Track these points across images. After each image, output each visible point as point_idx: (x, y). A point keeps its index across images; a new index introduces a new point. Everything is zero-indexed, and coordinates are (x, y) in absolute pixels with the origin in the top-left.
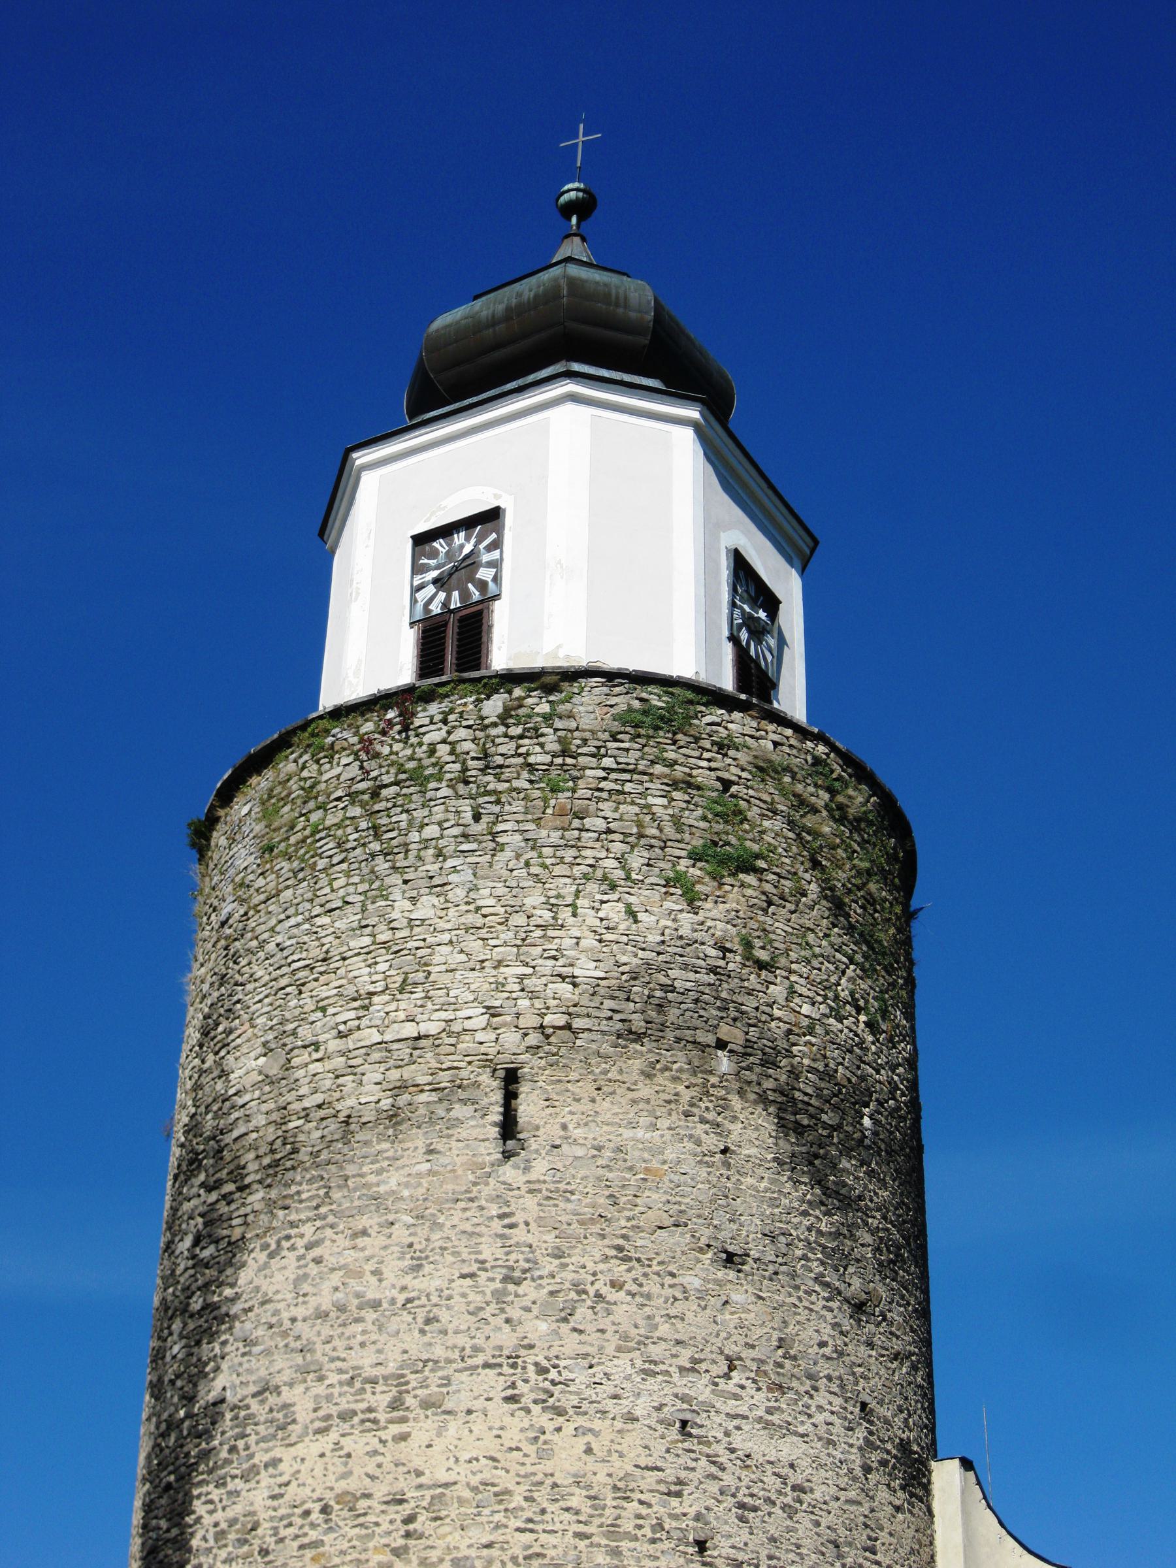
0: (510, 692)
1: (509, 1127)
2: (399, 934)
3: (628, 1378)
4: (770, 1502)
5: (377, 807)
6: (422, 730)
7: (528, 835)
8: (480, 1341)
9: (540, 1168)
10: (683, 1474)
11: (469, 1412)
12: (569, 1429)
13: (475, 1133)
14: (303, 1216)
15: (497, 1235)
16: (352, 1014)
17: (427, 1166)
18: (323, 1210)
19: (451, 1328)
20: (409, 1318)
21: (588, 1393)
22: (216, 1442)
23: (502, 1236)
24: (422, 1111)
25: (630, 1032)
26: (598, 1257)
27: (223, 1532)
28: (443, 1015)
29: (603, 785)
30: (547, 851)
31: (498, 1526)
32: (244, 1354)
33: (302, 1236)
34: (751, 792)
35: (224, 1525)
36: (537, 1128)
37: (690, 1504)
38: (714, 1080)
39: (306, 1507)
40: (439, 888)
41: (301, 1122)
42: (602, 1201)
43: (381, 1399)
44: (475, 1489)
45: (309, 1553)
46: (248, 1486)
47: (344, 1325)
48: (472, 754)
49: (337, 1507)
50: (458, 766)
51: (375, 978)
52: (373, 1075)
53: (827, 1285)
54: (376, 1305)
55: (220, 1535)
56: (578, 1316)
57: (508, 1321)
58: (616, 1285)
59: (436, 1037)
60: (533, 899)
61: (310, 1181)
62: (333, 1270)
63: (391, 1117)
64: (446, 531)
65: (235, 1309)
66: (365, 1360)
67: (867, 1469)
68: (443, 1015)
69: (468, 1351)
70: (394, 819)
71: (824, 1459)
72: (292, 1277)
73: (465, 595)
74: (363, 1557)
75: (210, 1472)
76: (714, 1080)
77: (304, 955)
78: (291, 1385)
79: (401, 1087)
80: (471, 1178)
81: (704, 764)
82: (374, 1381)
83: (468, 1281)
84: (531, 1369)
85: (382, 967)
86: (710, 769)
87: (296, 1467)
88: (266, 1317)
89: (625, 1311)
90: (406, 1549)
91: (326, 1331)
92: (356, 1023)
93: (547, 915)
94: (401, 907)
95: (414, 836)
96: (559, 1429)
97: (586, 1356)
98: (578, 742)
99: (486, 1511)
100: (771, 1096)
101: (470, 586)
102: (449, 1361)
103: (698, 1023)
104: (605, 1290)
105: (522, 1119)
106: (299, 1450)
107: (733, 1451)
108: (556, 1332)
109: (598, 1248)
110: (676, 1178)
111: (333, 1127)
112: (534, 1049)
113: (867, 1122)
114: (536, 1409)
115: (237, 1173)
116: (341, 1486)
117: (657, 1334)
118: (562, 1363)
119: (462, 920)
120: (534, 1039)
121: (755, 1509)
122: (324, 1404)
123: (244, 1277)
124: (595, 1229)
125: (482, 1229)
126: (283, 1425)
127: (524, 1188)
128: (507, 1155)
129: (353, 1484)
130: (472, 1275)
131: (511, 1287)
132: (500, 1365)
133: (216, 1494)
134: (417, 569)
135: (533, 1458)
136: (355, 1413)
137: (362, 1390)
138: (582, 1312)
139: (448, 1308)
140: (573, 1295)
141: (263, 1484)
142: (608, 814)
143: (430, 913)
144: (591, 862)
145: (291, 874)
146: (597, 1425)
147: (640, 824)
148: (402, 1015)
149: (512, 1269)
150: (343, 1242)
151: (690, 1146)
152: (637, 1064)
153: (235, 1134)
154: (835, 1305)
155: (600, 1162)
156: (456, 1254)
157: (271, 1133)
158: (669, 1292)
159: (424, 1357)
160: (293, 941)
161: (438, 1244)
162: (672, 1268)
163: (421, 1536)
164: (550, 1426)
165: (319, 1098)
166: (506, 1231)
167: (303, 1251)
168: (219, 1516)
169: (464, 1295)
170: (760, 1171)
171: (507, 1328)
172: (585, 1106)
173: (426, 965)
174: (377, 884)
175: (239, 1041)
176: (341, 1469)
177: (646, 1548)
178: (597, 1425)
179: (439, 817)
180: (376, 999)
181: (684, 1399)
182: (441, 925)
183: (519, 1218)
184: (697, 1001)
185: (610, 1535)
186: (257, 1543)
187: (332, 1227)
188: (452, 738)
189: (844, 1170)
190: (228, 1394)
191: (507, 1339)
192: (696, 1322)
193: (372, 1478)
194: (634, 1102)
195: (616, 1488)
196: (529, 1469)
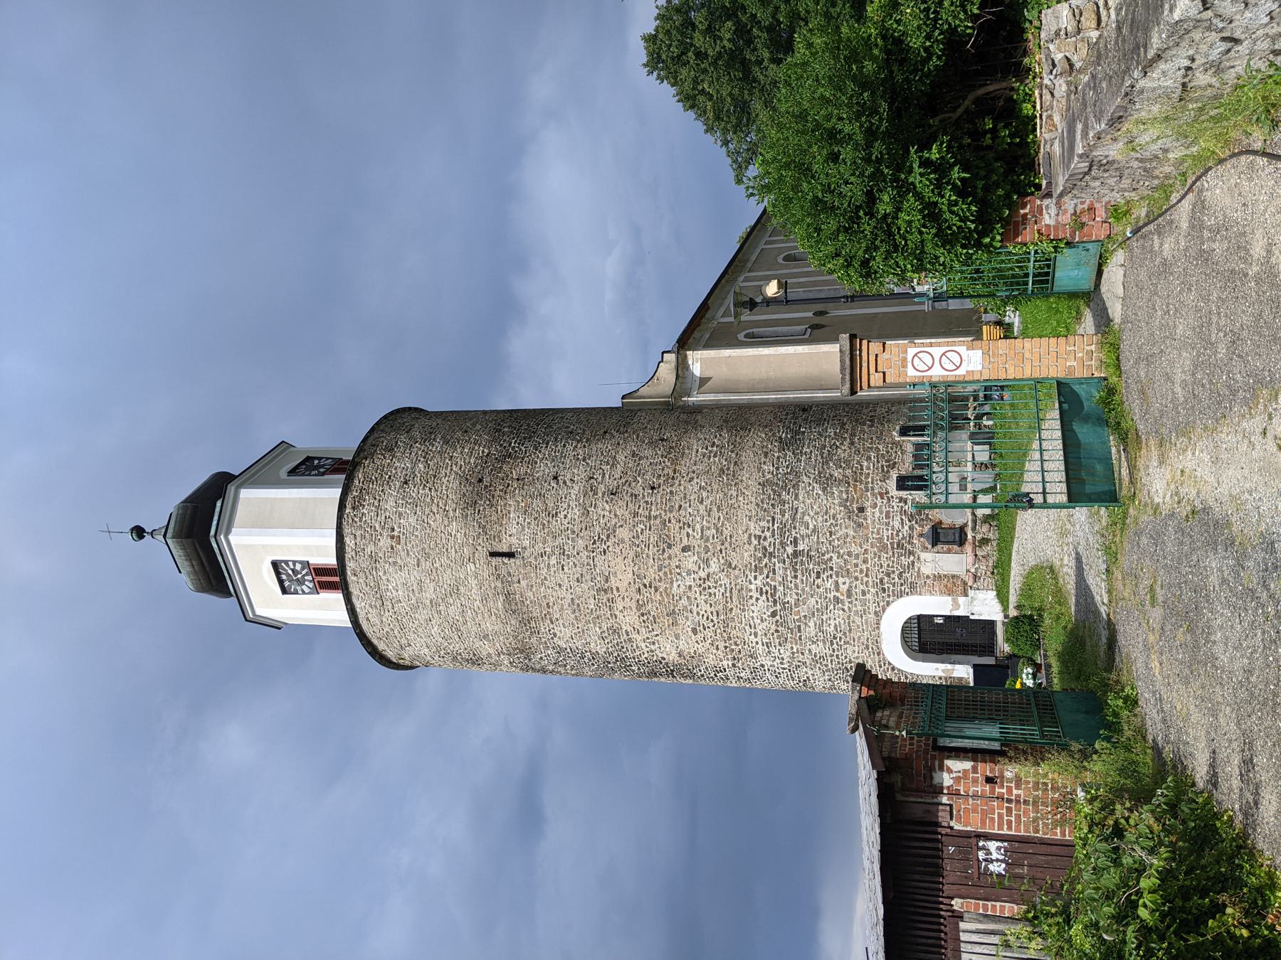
1: (510, 555)
15: (549, 558)
16: (469, 611)
44: (635, 564)
58: (566, 517)
64: (281, 582)
90: (655, 587)
105: (508, 550)
107: (621, 477)
108: (582, 538)
114: (608, 544)
116: (634, 609)
126: (615, 631)
129: (634, 605)
131: (566, 553)
134: (296, 593)
176: (629, 610)
193: (631, 599)
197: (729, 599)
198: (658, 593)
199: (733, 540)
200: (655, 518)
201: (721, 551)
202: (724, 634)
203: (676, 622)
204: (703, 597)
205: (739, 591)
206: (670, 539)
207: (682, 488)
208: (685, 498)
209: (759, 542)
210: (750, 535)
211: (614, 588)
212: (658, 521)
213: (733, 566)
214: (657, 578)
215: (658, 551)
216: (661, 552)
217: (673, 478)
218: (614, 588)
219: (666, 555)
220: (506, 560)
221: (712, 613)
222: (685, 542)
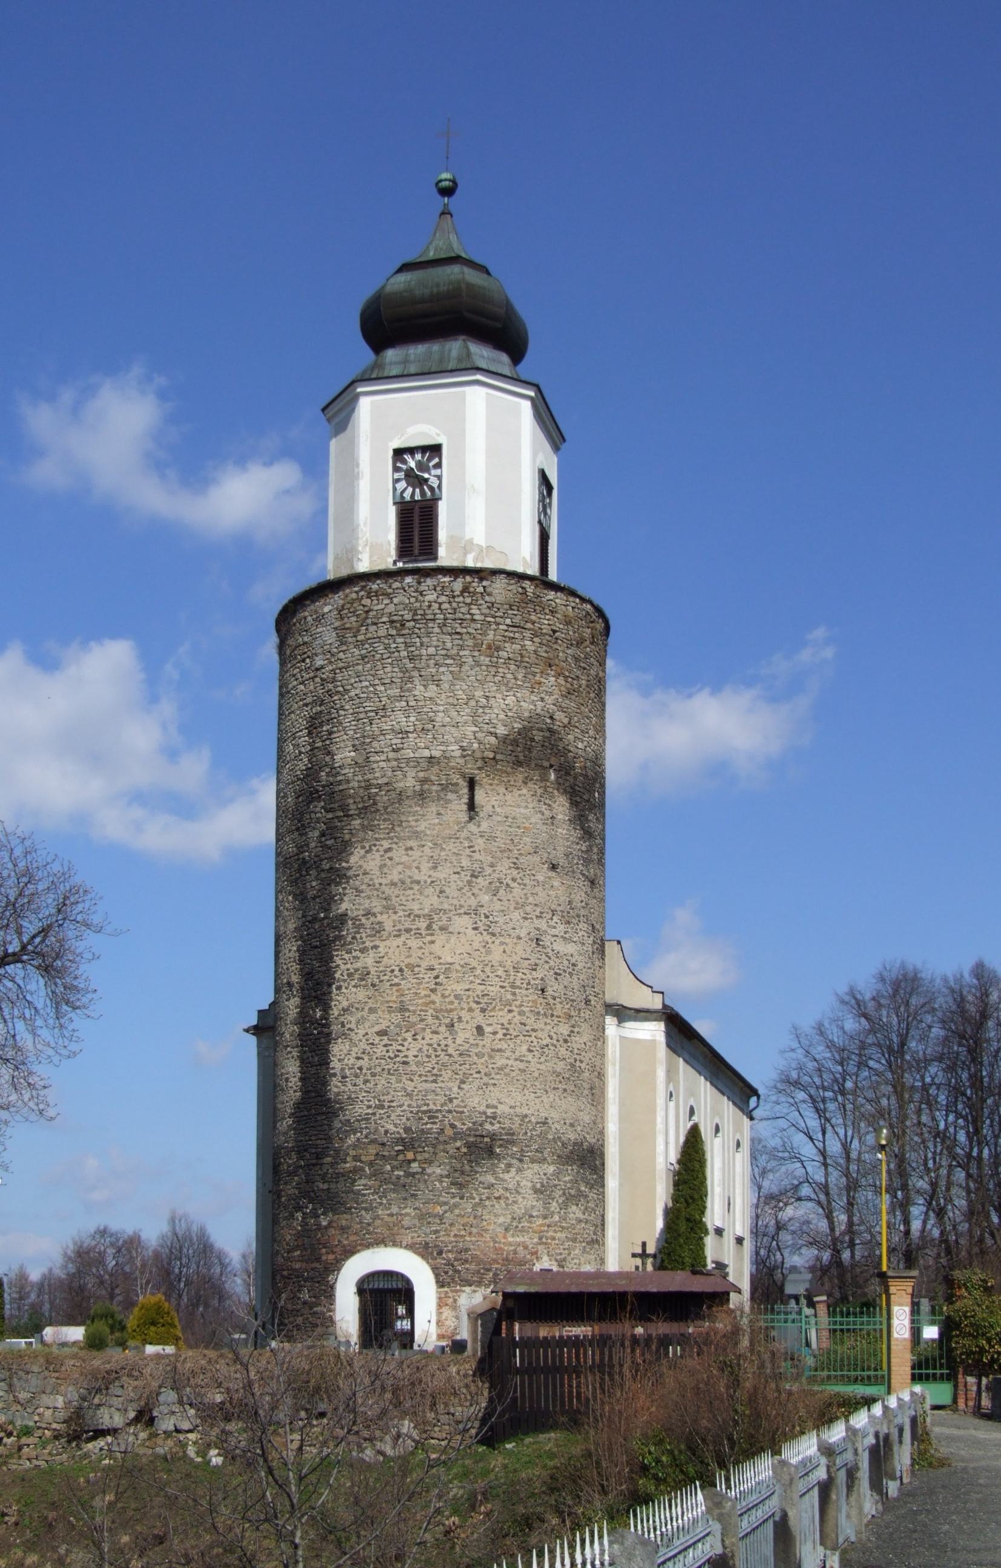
0: (464, 578)
1: (471, 806)
2: (420, 704)
3: (518, 921)
4: (565, 971)
5: (404, 632)
6: (424, 593)
7: (475, 659)
8: (462, 903)
9: (485, 825)
10: (537, 961)
11: (459, 933)
12: (497, 942)
13: (458, 807)
14: (382, 836)
16: (399, 741)
17: (438, 820)
18: (392, 834)
19: (450, 896)
20: (433, 890)
21: (504, 927)
22: (344, 933)
23: (470, 856)
24: (434, 794)
25: (518, 762)
26: (507, 868)
27: (352, 973)
28: (442, 748)
29: (506, 634)
30: (484, 668)
31: (471, 982)
32: (356, 896)
33: (382, 846)
34: (563, 636)
35: (352, 971)
36: (483, 807)
37: (539, 974)
38: (548, 784)
39: (394, 968)
40: (438, 683)
41: (377, 790)
42: (508, 841)
43: (423, 924)
44: (462, 966)
45: (395, 988)
46: (363, 955)
47: (404, 890)
48: (450, 611)
49: (406, 970)
50: (442, 616)
51: (409, 724)
52: (411, 773)
53: (583, 875)
54: (418, 882)
55: (350, 975)
56: (500, 894)
57: (473, 894)
58: (514, 880)
59: (439, 759)
60: (479, 693)
61: (385, 820)
62: (398, 864)
63: (420, 795)
65: (350, 873)
66: (415, 907)
67: (593, 953)
68: (442, 748)
69: (458, 907)
70: (413, 640)
71: (582, 952)
72: (379, 864)
73: (423, 493)
74: (418, 991)
75: (342, 946)
76: (548, 784)
77: (372, 704)
78: (381, 914)
79: (424, 781)
80: (456, 828)
81: (546, 622)
82: (419, 916)
83: (457, 876)
84: (483, 916)
85: (412, 719)
86: (549, 625)
87: (386, 950)
88: (366, 881)
89: (518, 892)
91: (397, 892)
92: (401, 746)
93: (484, 701)
94: (419, 690)
95: (424, 652)
96: (493, 942)
97: (503, 911)
98: (495, 610)
99: (467, 976)
100: (569, 789)
101: (425, 487)
102: (450, 911)
103: (542, 756)
104: (510, 882)
106: (388, 943)
108: (492, 900)
109: (507, 863)
110: (535, 831)
111: (394, 796)
112: (480, 769)
113: (596, 795)
114: (485, 933)
115: (344, 808)
116: (407, 961)
117: (528, 901)
118: (495, 914)
119: (448, 700)
120: (480, 764)
121: (560, 975)
122: (397, 924)
123: (353, 860)
124: (506, 855)
125: (461, 852)
126: (378, 931)
127: (478, 834)
128: (471, 819)
129: (412, 961)
130: (458, 873)
131: (474, 879)
132: (470, 914)
133: (346, 956)
135: (484, 955)
136: (411, 930)
137: (414, 920)
138: (502, 892)
139: (449, 887)
140: (498, 884)
141: (371, 956)
142: (508, 649)
143: (434, 695)
144: (502, 675)
145: (360, 657)
146: (507, 940)
147: (522, 656)
148: (423, 745)
149: (474, 871)
151: (541, 816)
152: (520, 777)
153: (341, 788)
154: (585, 883)
155: (507, 824)
156: (451, 863)
158: (532, 883)
159: (440, 908)
160: (365, 695)
161: (444, 858)
162: (533, 872)
163: (441, 985)
164: (490, 941)
165: (385, 780)
166: (471, 854)
167: (382, 853)
168: (349, 966)
169: (455, 882)
170: (564, 825)
171: (473, 898)
172: (501, 797)
173: (433, 721)
174: (407, 675)
175: (338, 740)
177: (524, 992)
178: (507, 940)
179: (435, 643)
180: (410, 735)
181: (538, 929)
182: (439, 702)
183: (476, 848)
184: (543, 746)
185: (513, 987)
186: (369, 980)
187: (396, 843)
188: (440, 600)
189: (591, 821)
190: (349, 912)
191: (473, 902)
193: (421, 958)
194: (520, 795)
195: (514, 967)
196: (483, 958)
197: (424, 1078)
198: (428, 992)
199: (491, 1088)
200: (514, 994)
201: (479, 1072)
202: (379, 1069)
203: (393, 1012)
204: (425, 1048)
205: (434, 1091)
206: (491, 1011)
207: (542, 1026)
208: (533, 1030)
209: (490, 1117)
210: (496, 1107)
211: (433, 938)
212: (509, 997)
213: (462, 1086)
214: (447, 993)
215: (478, 996)
216: (476, 999)
217: (552, 1015)
218: (433, 938)
219: (474, 1006)
221: (406, 1056)
222: (488, 1029)
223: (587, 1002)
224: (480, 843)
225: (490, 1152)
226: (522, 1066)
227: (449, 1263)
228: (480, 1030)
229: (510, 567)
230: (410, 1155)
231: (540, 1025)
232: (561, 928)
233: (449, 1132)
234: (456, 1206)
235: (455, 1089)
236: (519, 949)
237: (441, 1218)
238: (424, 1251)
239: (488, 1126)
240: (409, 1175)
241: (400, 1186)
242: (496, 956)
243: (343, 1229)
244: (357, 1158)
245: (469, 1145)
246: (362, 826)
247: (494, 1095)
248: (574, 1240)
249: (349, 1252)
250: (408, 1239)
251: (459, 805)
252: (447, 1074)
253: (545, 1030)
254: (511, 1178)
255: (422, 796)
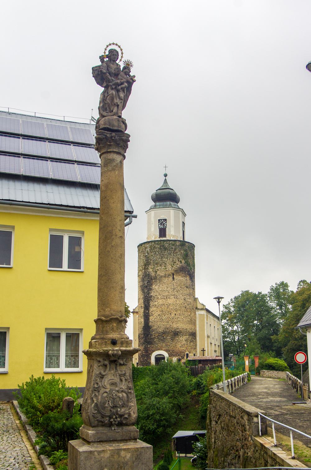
9: (176, 281)
43: (165, 297)
64: (161, 220)
66: (164, 294)
79: (165, 274)
89: (181, 292)
94: (164, 259)
128: (173, 280)
129: (164, 303)
134: (159, 223)
150: (162, 285)
152: (181, 273)
157: (154, 276)
191: (174, 294)
192: (185, 292)
220: (172, 277)
223: (193, 309)
224: (175, 284)
225: (178, 335)
226: (182, 320)
227: (171, 353)
228: (175, 314)
229: (178, 239)
230: (164, 335)
231: (185, 313)
232: (188, 297)
233: (170, 331)
234: (172, 343)
235: (171, 324)
236: (182, 301)
237: (169, 345)
238: (166, 351)
239: (177, 330)
240: (164, 338)
241: (162, 340)
242: (178, 302)
243: (152, 347)
244: (154, 336)
245: (174, 333)
246: (155, 281)
247: (178, 325)
248: (192, 348)
249: (154, 351)
250: (164, 349)
251: (171, 278)
252: (170, 322)
253: (186, 314)
254: (181, 338)
255: (165, 277)
